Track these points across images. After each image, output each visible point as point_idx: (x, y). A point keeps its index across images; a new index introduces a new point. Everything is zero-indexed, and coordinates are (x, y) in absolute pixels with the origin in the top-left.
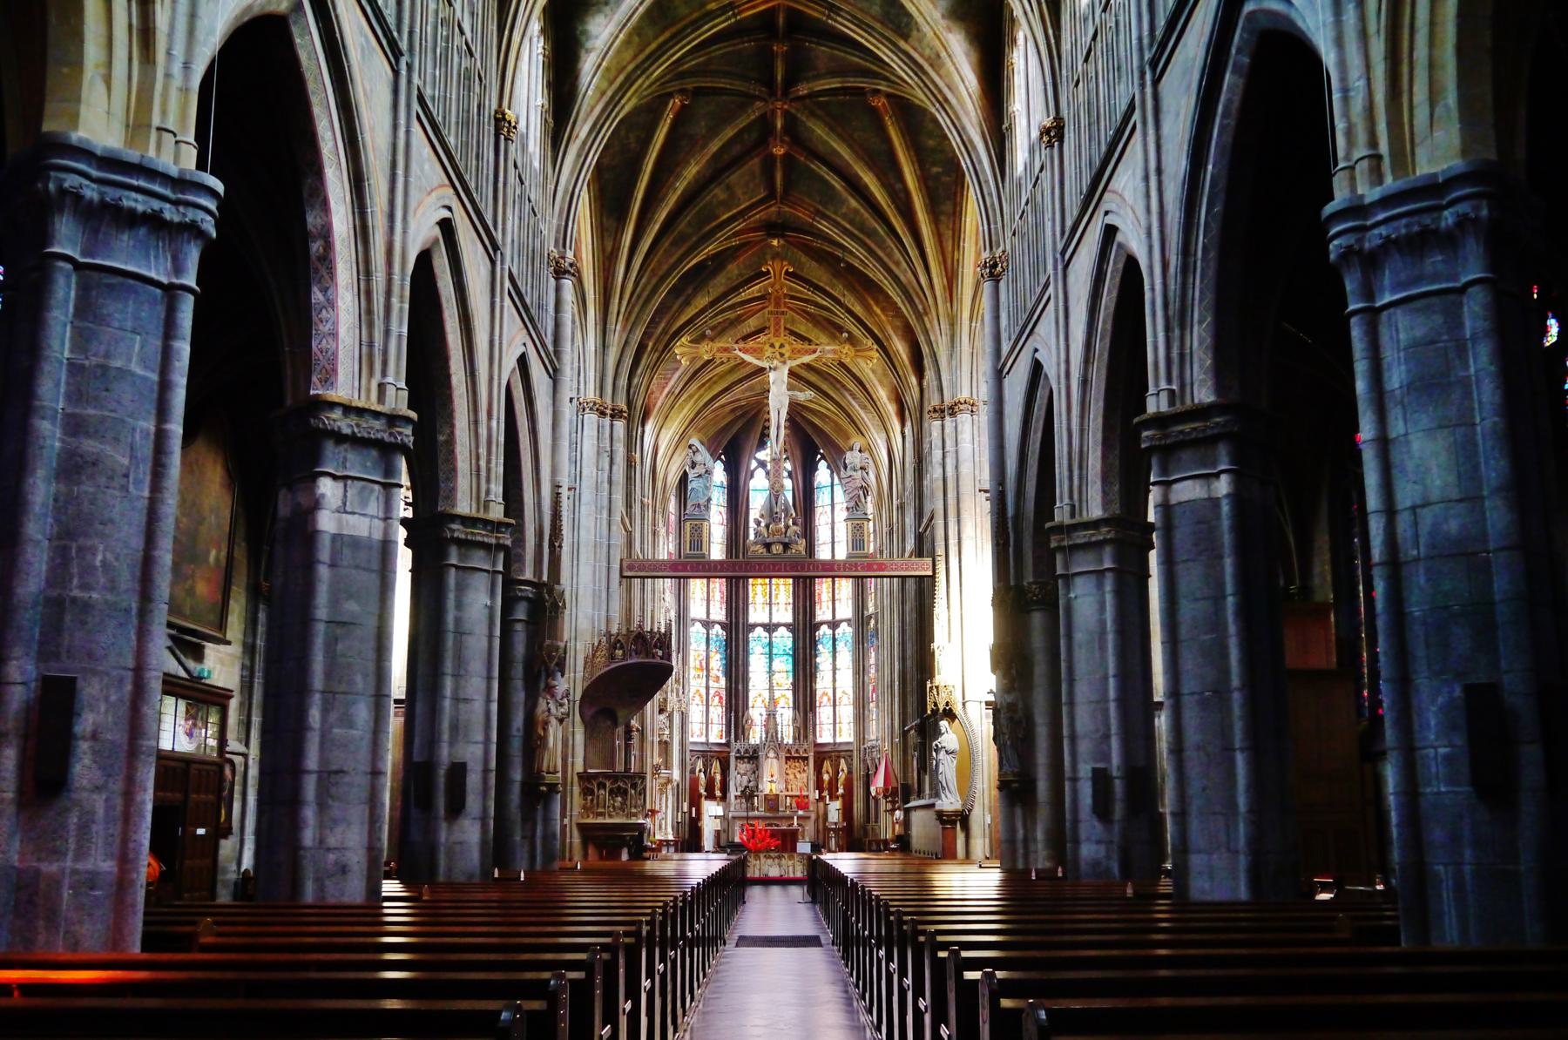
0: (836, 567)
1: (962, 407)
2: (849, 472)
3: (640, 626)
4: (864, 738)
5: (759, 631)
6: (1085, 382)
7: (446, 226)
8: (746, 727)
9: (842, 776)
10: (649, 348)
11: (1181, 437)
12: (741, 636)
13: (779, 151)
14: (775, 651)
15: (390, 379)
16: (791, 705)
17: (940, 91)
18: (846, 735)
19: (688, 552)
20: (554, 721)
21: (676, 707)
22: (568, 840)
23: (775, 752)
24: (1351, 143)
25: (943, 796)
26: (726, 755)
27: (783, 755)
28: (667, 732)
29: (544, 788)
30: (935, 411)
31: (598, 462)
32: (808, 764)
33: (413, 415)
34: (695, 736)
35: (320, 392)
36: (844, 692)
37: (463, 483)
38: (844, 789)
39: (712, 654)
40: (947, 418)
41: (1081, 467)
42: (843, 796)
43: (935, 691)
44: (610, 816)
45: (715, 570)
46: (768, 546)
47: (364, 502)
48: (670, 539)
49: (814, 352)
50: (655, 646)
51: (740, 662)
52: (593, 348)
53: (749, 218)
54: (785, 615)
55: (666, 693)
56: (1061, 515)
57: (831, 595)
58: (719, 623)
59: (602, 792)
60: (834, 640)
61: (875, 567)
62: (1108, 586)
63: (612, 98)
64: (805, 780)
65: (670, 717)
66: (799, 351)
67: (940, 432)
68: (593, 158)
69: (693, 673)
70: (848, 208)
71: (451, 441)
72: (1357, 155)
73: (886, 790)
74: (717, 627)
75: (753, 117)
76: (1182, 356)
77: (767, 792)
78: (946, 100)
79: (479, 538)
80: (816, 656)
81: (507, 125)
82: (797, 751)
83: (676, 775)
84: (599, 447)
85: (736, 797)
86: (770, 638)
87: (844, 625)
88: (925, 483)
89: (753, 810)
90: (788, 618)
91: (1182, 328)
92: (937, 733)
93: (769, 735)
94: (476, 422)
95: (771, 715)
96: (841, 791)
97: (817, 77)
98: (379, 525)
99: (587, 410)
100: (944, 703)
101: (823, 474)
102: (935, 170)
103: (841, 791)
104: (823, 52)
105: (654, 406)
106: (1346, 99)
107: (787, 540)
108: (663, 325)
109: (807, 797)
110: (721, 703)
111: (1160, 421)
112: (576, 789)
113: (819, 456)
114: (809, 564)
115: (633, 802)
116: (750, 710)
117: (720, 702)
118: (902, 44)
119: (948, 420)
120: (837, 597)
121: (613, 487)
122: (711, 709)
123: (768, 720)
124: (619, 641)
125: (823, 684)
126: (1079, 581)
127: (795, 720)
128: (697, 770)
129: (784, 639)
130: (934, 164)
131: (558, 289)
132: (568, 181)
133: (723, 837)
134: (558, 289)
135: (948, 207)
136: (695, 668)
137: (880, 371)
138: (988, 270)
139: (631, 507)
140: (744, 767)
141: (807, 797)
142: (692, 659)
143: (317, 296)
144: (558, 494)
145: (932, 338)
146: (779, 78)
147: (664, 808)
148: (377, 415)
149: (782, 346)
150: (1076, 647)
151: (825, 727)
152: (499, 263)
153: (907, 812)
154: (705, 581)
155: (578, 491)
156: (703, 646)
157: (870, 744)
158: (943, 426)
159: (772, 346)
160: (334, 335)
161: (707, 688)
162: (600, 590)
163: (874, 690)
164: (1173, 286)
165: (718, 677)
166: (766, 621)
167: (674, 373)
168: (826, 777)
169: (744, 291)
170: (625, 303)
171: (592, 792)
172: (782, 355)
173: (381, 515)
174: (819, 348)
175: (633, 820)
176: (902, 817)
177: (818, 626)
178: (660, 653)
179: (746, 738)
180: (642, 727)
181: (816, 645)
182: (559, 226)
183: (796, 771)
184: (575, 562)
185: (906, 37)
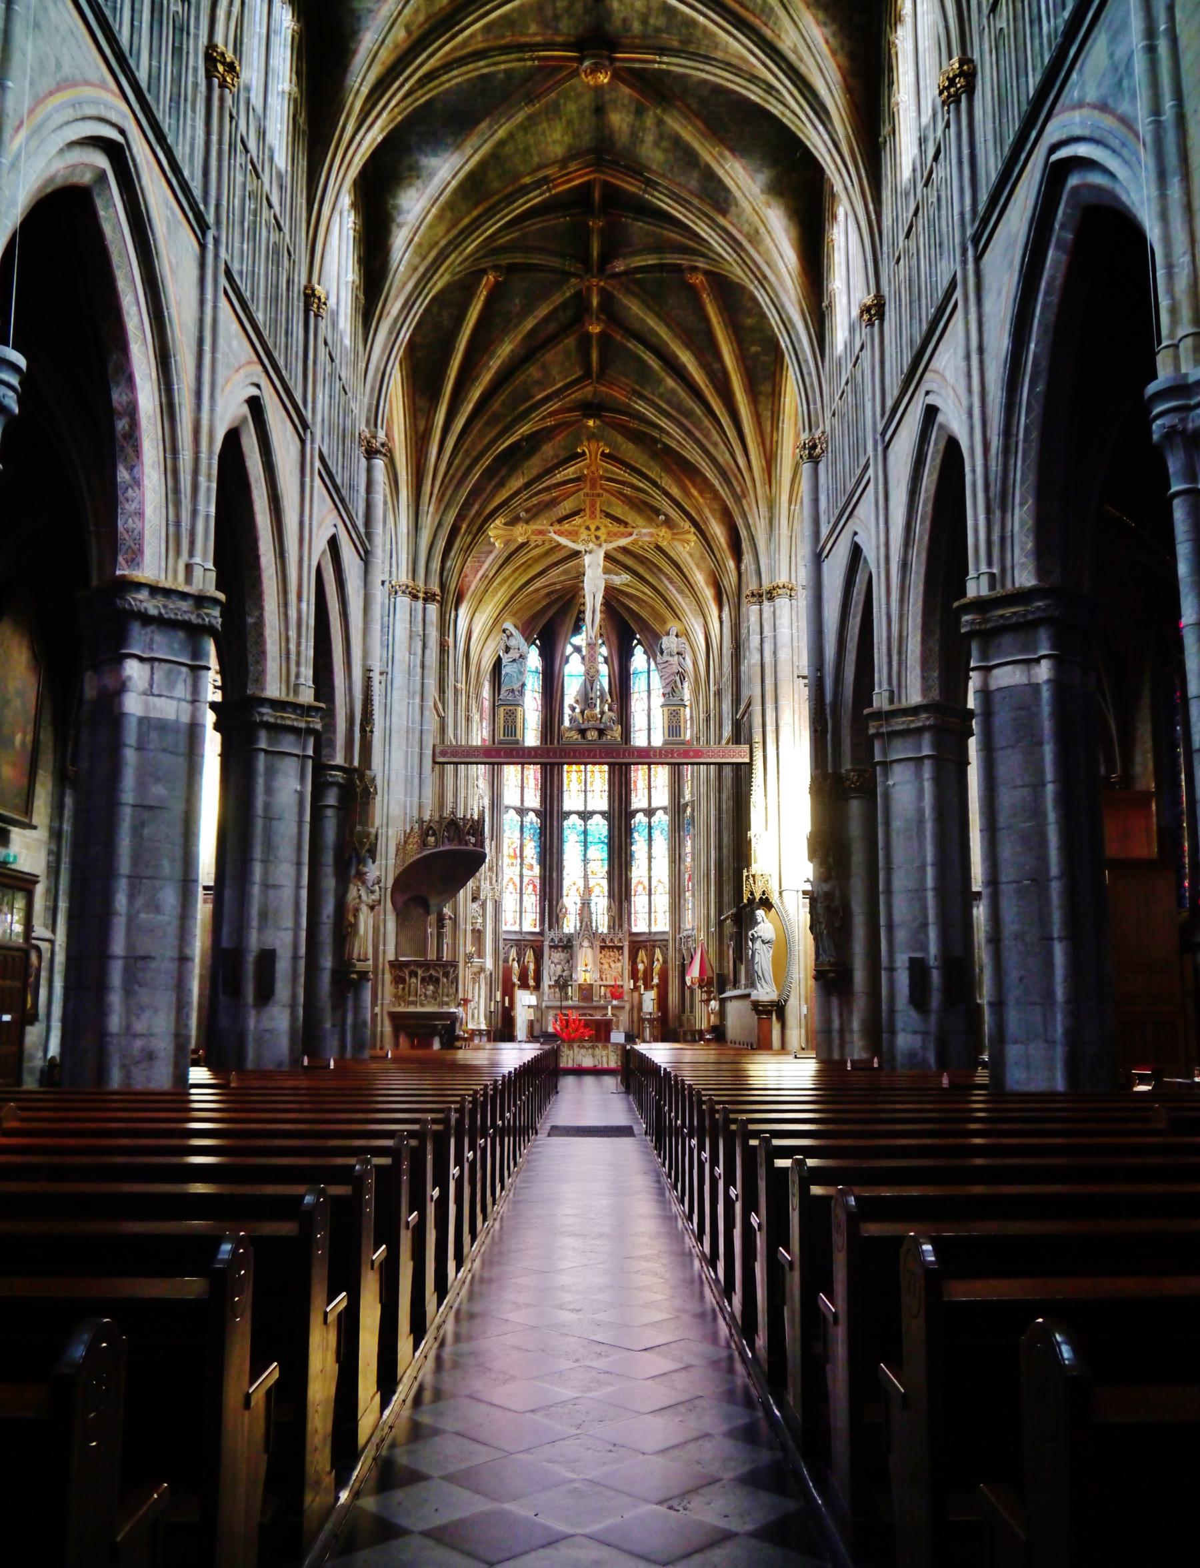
0: (652, 753)
1: (780, 591)
2: (666, 658)
3: (453, 813)
4: (680, 927)
5: (574, 818)
6: (905, 566)
7: (255, 404)
8: (560, 915)
9: (657, 966)
10: (463, 531)
11: (1002, 621)
12: (555, 824)
13: (595, 329)
14: (590, 839)
15: (197, 559)
16: (606, 894)
17: (759, 268)
18: (662, 924)
19: (502, 737)
20: (364, 908)
21: (489, 895)
22: (379, 1029)
23: (590, 941)
24: (1174, 322)
25: (759, 985)
26: (539, 944)
27: (598, 944)
28: (480, 921)
29: (354, 976)
30: (753, 595)
31: (410, 646)
32: (622, 954)
33: (221, 596)
34: (508, 924)
35: (126, 573)
36: (660, 881)
37: (273, 666)
38: (659, 979)
40: (766, 603)
41: (900, 653)
42: (658, 986)
43: (751, 879)
44: (422, 1005)
45: (529, 756)
46: (583, 732)
47: (172, 685)
48: (484, 725)
49: (631, 534)
50: (468, 833)
51: (555, 850)
52: (405, 531)
53: (564, 398)
54: (600, 802)
55: (480, 881)
56: (880, 701)
57: (646, 782)
58: (533, 811)
59: (413, 980)
60: (650, 828)
61: (692, 754)
62: (927, 771)
63: (424, 274)
65: (483, 906)
66: (615, 534)
67: (758, 616)
68: (405, 335)
69: (506, 861)
70: (666, 388)
71: (260, 624)
72: (1181, 333)
73: (701, 980)
74: (532, 815)
75: (568, 294)
76: (1003, 539)
77: (581, 981)
78: (765, 277)
79: (289, 722)
80: (631, 844)
81: (316, 301)
83: (489, 964)
84: (411, 631)
85: (550, 986)
86: (585, 825)
87: (660, 813)
88: (742, 668)
89: (567, 999)
90: (604, 806)
91: (1004, 510)
92: (754, 922)
93: (584, 924)
94: (286, 605)
95: (586, 904)
96: (656, 981)
97: (634, 253)
98: (186, 707)
99: (400, 593)
100: (760, 892)
101: (639, 659)
102: (754, 349)
103: (656, 981)
104: (639, 227)
105: (468, 589)
106: (1170, 276)
107: (602, 726)
108: (476, 507)
109: (622, 986)
111: (980, 605)
112: (388, 977)
113: (635, 642)
114: (624, 751)
115: (445, 990)
116: (565, 898)
117: (534, 890)
118: (721, 220)
120: (652, 784)
121: (426, 672)
122: (525, 897)
123: (582, 909)
124: (431, 828)
125: (638, 872)
126: (897, 769)
127: (609, 909)
128: (511, 958)
129: (600, 826)
130: (753, 344)
131: (369, 470)
132: (380, 360)
133: (537, 1027)
134: (369, 470)
135: (766, 388)
136: (509, 856)
137: (697, 555)
138: (807, 452)
139: (444, 692)
140: (558, 956)
141: (622, 986)
143: (123, 474)
144: (370, 678)
145: (751, 521)
146: (595, 253)
147: (476, 998)
148: (184, 596)
149: (598, 528)
150: (894, 835)
152: (308, 442)
153: (723, 1002)
154: (519, 767)
155: (390, 676)
157: (685, 933)
158: (761, 610)
159: (588, 528)
160: (140, 514)
161: (521, 876)
162: (412, 777)
163: (690, 878)
164: (995, 467)
165: (532, 866)
166: (581, 808)
167: (487, 557)
168: (641, 967)
169: (560, 472)
170: (438, 484)
171: (403, 981)
172: (597, 538)
173: (189, 697)
174: (636, 531)
175: (445, 1009)
176: (717, 1008)
177: (632, 814)
178: (473, 840)
179: (560, 927)
180: (455, 915)
181: (631, 833)
182: (370, 405)
183: (610, 961)
184: (387, 748)
185: (724, 213)
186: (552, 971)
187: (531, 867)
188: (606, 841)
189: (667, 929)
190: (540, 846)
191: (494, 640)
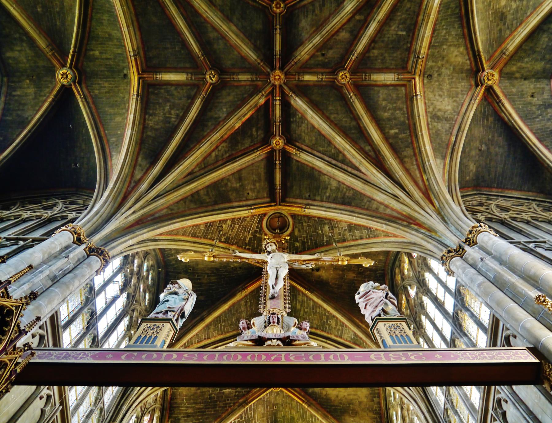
70: (331, 190)
102: (392, 132)
119: (471, 252)
130: (392, 128)
135: (409, 152)
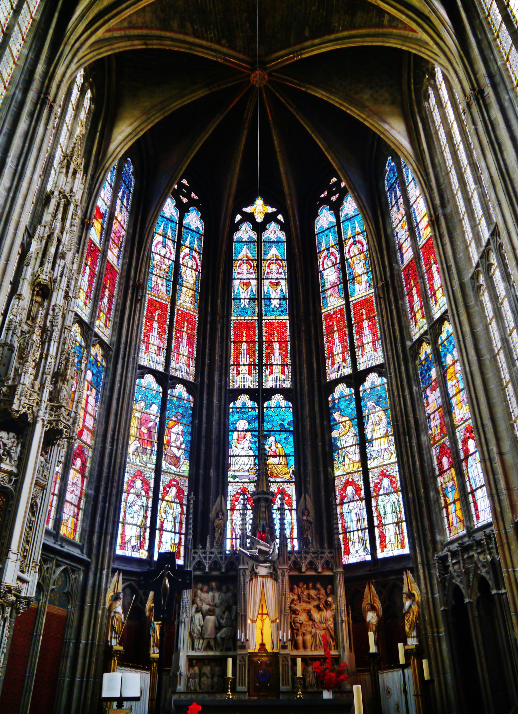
4: (434, 541)
5: (244, 399)
14: (267, 426)
16: (294, 506)
32: (333, 593)
34: (129, 546)
39: (171, 423)
57: (347, 344)
60: (359, 400)
64: (331, 624)
69: (133, 445)
77: (254, 647)
80: (331, 429)
82: (312, 566)
85: (191, 660)
86: (261, 408)
90: (287, 383)
109: (337, 659)
110: (181, 499)
116: (229, 513)
122: (162, 505)
136: (140, 439)
141: (337, 659)
142: (134, 423)
151: (354, 536)
156: (155, 409)
161: (158, 471)
163: (443, 451)
166: (254, 385)
181: (330, 414)
186: (197, 628)
187: (176, 461)
188: (292, 429)
189: (406, 551)
190: (192, 434)
191: (131, 125)
